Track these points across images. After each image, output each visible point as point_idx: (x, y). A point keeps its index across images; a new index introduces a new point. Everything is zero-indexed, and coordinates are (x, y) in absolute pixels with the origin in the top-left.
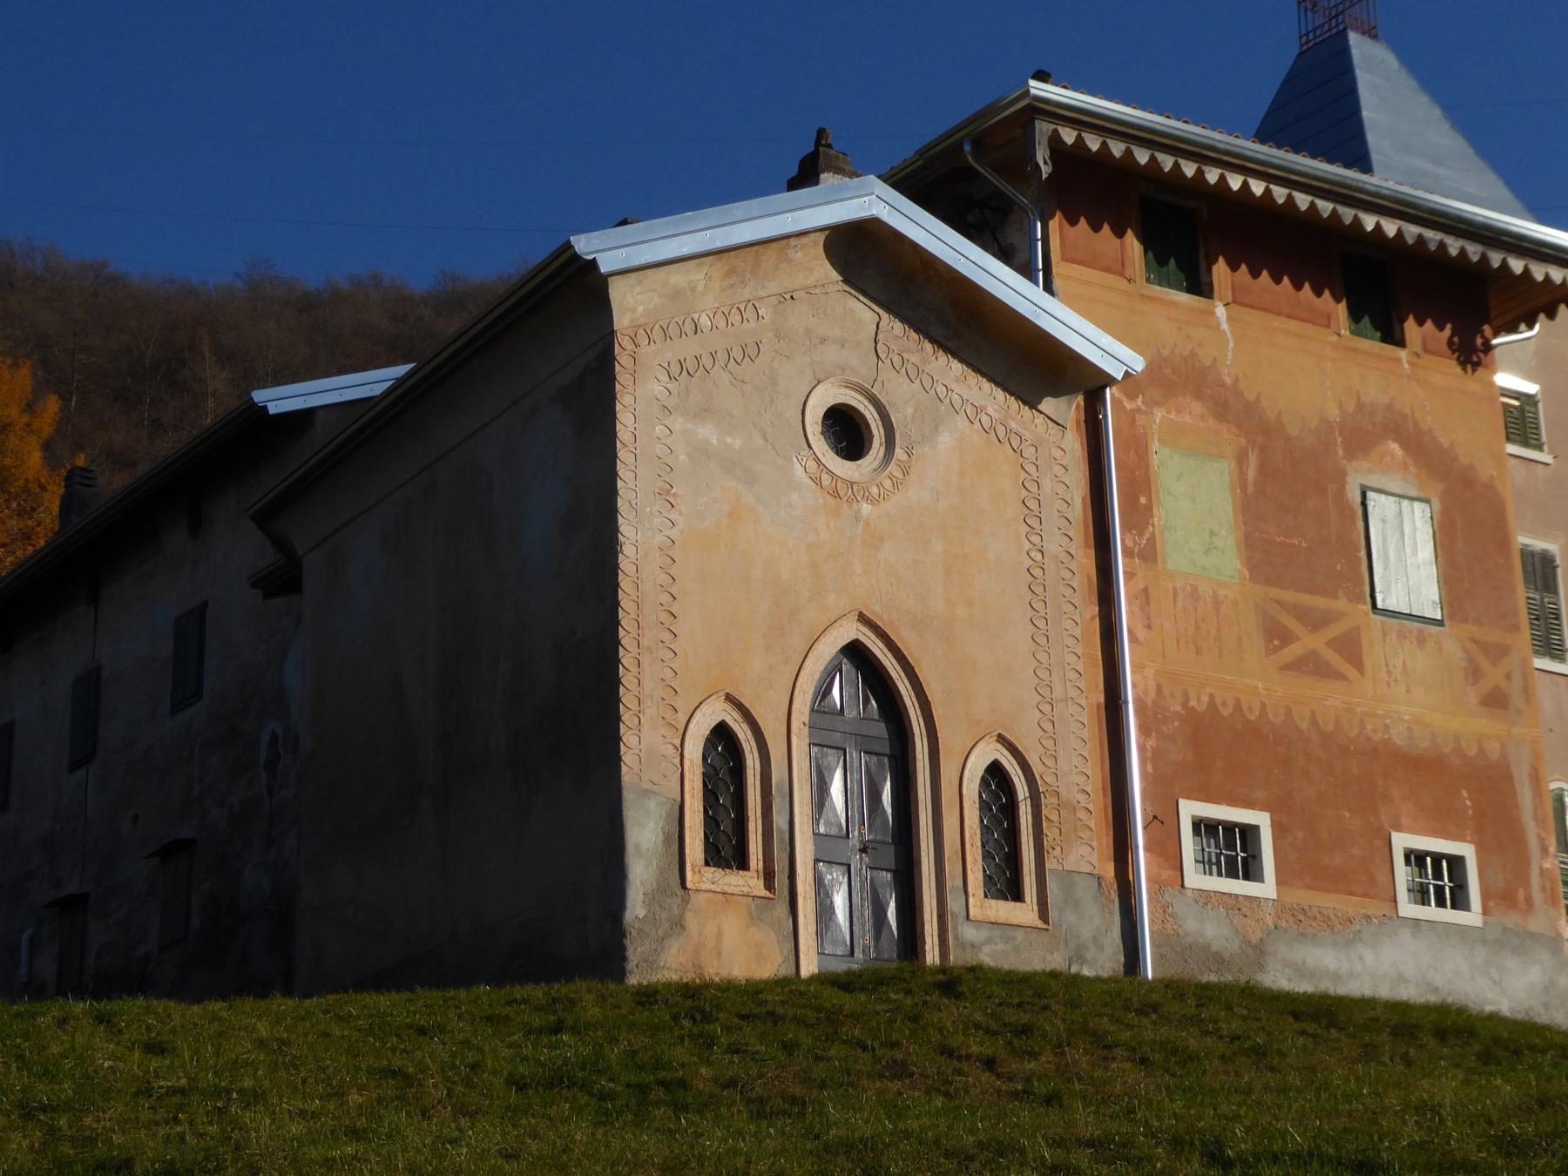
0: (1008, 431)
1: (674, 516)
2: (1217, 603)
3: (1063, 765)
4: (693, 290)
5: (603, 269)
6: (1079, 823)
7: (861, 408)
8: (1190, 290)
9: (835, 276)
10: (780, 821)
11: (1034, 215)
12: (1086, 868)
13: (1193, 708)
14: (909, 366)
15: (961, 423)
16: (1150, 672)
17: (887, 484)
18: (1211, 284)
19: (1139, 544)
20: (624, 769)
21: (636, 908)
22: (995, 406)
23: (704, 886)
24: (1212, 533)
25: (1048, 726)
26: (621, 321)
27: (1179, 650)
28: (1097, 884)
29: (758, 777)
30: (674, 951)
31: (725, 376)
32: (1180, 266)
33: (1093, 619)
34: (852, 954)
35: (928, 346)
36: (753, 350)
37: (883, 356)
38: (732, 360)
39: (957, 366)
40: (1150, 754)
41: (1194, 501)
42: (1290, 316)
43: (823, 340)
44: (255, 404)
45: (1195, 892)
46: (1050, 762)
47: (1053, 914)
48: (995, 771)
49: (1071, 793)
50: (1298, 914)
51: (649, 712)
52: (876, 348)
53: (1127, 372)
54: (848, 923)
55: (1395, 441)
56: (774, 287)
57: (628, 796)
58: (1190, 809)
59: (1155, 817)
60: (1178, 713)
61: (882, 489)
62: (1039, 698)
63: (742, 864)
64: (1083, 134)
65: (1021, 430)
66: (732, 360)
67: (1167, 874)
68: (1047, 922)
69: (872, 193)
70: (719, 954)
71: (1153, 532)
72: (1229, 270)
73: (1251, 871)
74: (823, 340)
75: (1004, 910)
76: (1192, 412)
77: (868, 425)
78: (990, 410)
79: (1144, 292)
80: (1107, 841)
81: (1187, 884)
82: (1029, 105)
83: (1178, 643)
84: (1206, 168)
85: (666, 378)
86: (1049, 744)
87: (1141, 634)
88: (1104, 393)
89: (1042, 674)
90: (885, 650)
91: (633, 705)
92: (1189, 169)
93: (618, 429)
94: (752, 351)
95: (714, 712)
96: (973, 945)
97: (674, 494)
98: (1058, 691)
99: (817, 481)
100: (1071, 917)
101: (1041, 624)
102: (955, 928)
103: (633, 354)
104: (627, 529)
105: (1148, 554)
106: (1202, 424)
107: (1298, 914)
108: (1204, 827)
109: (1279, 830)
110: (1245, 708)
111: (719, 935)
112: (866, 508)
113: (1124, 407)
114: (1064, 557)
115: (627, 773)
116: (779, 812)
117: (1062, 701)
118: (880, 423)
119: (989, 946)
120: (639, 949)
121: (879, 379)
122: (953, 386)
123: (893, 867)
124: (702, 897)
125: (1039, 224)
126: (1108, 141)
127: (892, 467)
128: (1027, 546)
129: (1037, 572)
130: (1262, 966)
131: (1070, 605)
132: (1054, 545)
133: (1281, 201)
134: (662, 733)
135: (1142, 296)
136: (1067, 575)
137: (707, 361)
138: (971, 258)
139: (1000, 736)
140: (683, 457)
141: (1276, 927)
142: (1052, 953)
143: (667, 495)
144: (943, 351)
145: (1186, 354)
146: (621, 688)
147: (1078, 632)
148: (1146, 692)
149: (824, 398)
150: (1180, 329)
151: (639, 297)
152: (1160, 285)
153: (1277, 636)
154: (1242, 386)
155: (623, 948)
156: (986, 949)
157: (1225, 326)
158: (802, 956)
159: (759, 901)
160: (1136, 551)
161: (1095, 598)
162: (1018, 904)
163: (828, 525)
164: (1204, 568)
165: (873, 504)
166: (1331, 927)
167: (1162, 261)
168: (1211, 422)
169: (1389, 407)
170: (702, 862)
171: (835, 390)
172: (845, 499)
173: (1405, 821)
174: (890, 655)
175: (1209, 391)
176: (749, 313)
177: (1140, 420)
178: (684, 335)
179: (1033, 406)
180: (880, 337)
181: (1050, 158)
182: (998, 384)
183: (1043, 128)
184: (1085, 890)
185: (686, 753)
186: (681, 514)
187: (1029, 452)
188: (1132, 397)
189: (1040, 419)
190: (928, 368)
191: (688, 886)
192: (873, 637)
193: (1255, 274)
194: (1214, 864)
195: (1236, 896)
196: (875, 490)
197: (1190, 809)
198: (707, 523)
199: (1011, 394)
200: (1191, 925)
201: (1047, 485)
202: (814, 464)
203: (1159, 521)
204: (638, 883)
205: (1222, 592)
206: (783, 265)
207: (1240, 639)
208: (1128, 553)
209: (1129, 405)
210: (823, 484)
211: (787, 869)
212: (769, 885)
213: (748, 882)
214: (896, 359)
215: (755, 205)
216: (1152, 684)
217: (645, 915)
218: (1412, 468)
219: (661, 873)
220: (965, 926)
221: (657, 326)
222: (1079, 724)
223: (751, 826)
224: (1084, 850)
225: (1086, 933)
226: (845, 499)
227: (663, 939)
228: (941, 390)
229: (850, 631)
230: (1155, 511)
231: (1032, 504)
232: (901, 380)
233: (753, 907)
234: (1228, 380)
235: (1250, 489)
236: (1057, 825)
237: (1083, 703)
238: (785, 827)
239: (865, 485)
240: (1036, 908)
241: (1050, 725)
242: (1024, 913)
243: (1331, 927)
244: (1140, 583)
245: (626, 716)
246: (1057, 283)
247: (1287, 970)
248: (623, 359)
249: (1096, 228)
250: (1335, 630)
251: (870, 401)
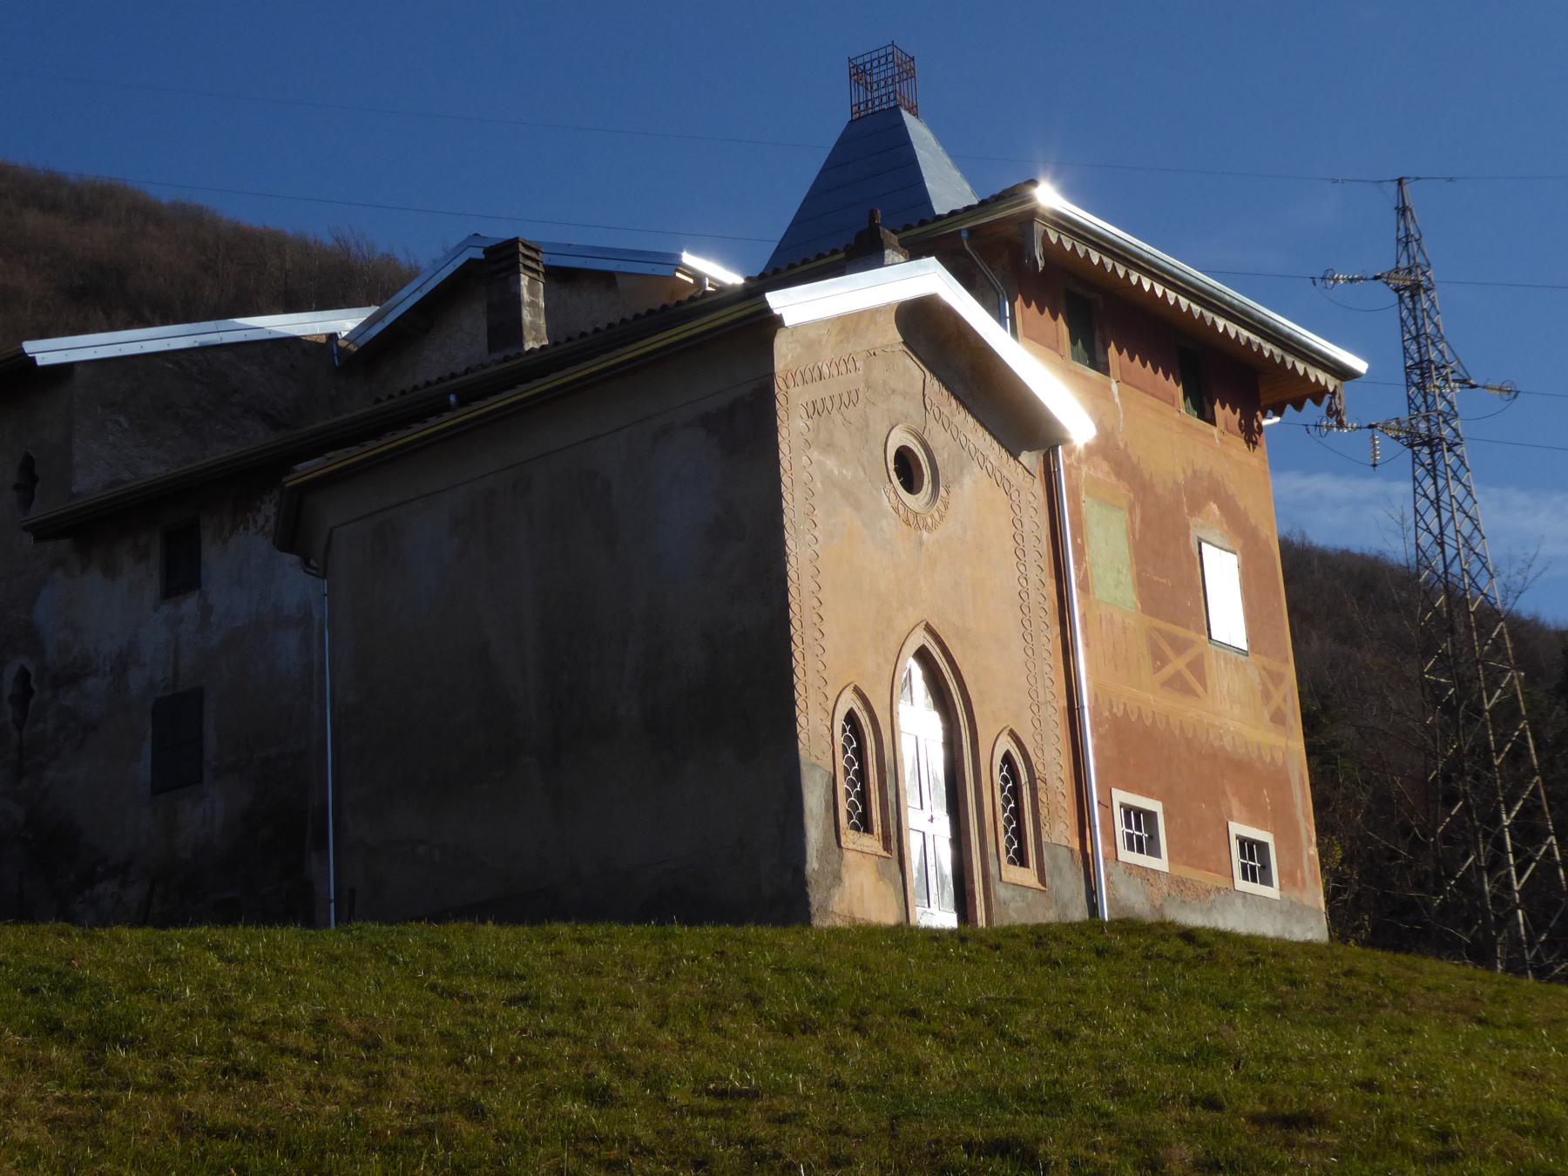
0: (1002, 477)
2: (1125, 629)
4: (820, 342)
7: (916, 450)
11: (1003, 296)
12: (1064, 842)
20: (800, 745)
21: (813, 864)
31: (839, 417)
33: (1057, 637)
36: (852, 398)
37: (929, 408)
42: (1152, 395)
44: (24, 354)
46: (1040, 754)
47: (1048, 879)
55: (1214, 502)
57: (804, 768)
65: (1010, 478)
78: (991, 459)
81: (1120, 858)
84: (1130, 271)
95: (849, 702)
98: (1041, 699)
99: (896, 510)
102: (994, 888)
118: (927, 464)
121: (928, 427)
125: (1007, 304)
132: (1034, 574)
147: (1049, 647)
149: (899, 438)
153: (1159, 659)
155: (806, 895)
159: (882, 859)
161: (1058, 622)
169: (1210, 474)
173: (1235, 813)
176: (851, 365)
182: (995, 438)
197: (1120, 796)
212: (887, 847)
213: (872, 843)
214: (936, 411)
218: (1225, 526)
219: (825, 833)
221: (798, 371)
234: (1122, 445)
235: (1137, 537)
238: (894, 800)
250: (1190, 655)
251: (921, 445)
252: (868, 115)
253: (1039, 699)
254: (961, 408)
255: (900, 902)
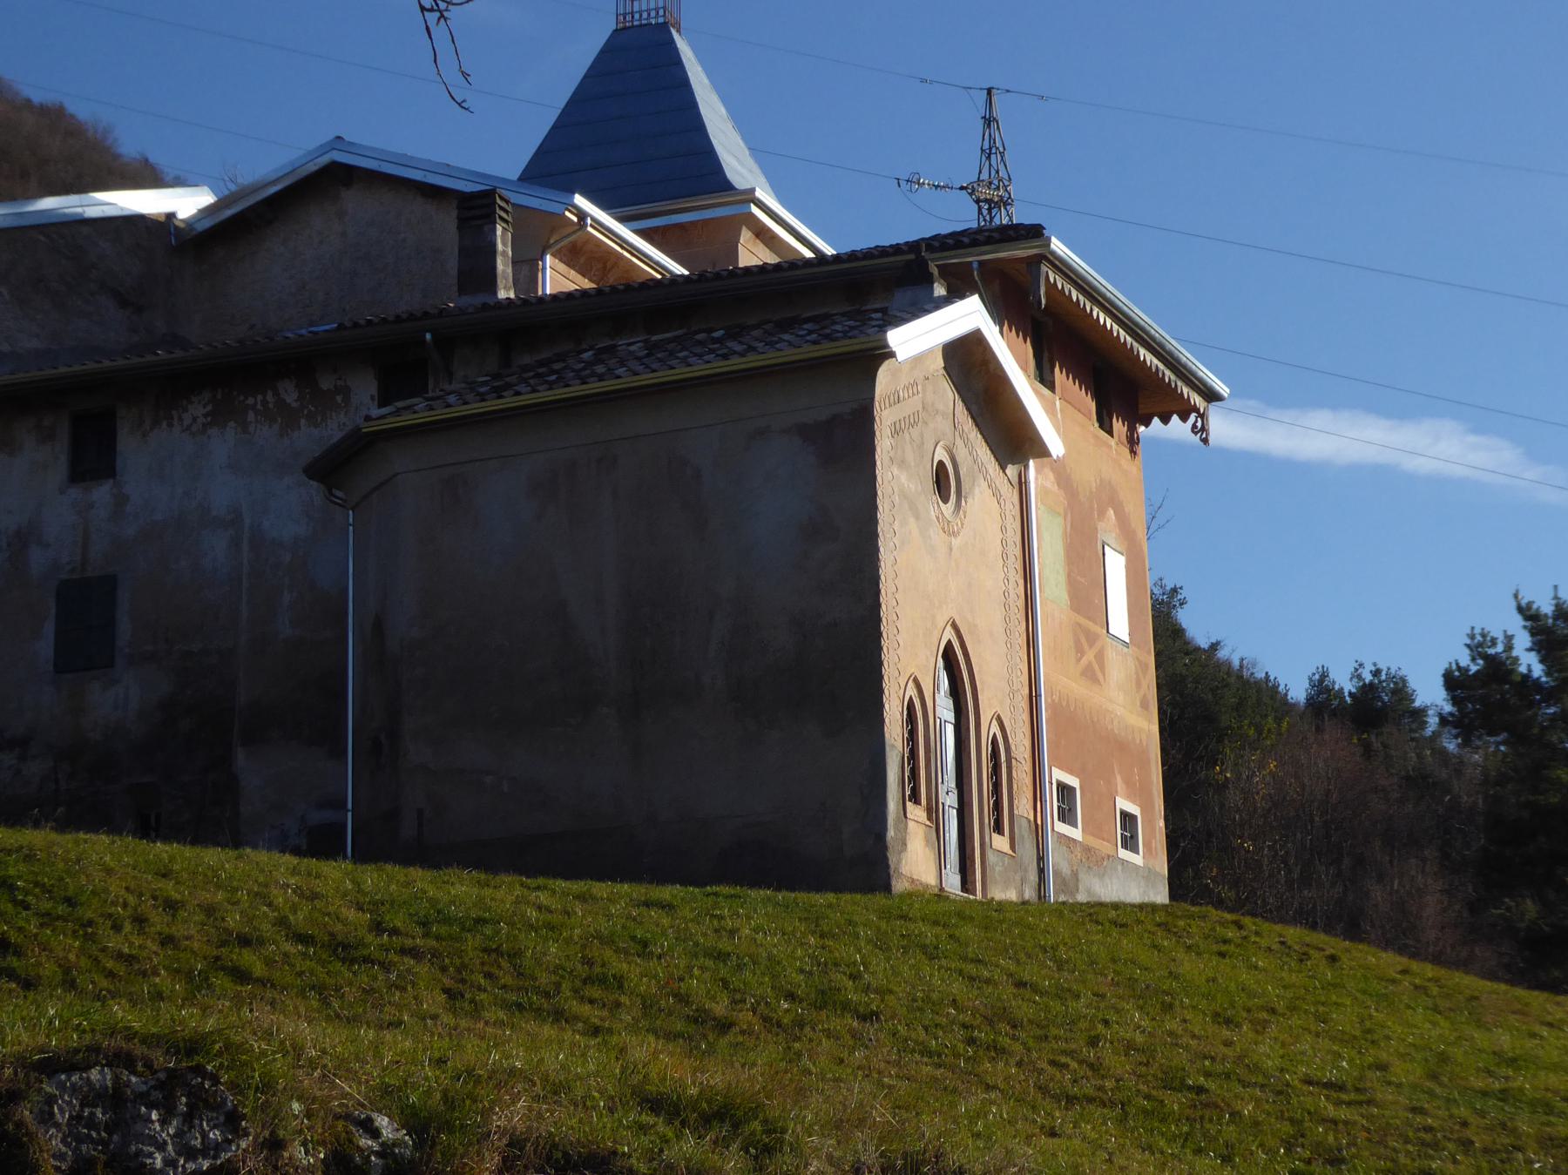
7: (947, 464)
46: (1013, 737)
57: (888, 748)
99: (938, 518)
149: (941, 455)
155: (886, 859)
212: (929, 818)
252: (633, 26)
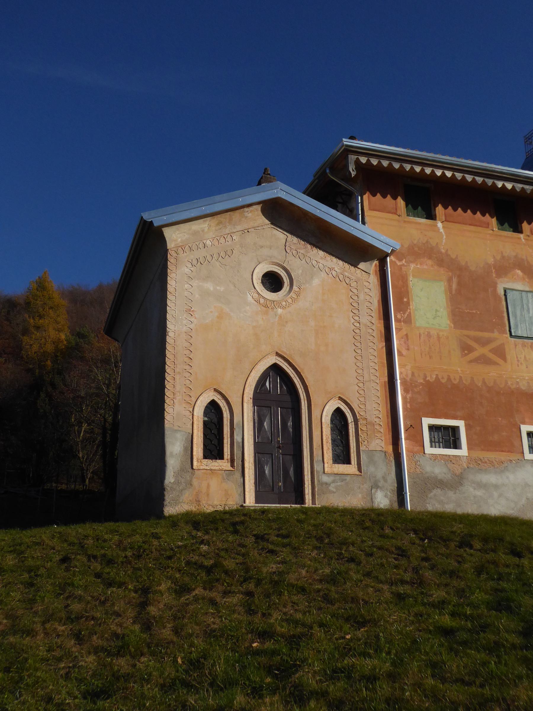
1: (192, 319)
2: (439, 338)
3: (368, 407)
4: (203, 231)
5: (156, 224)
6: (376, 430)
7: (279, 272)
8: (427, 218)
9: (267, 222)
10: (237, 438)
12: (379, 449)
13: (429, 380)
14: (300, 254)
15: (323, 275)
16: (408, 367)
17: (290, 301)
18: (435, 215)
19: (404, 317)
20: (166, 422)
21: (170, 478)
22: (339, 267)
23: (201, 467)
24: (437, 311)
25: (362, 392)
26: (170, 245)
27: (422, 357)
28: (384, 455)
29: (229, 421)
30: (187, 495)
31: (218, 264)
32: (423, 209)
33: (382, 348)
34: (273, 490)
35: (309, 246)
36: (229, 253)
38: (220, 257)
39: (321, 253)
40: (408, 400)
41: (428, 299)
42: (470, 225)
43: (262, 247)
45: (430, 455)
47: (363, 468)
48: (338, 412)
49: (371, 418)
50: (478, 462)
51: (179, 397)
52: (285, 248)
53: (392, 250)
54: (271, 477)
55: (518, 269)
56: (239, 228)
57: (167, 433)
58: (427, 422)
59: (411, 426)
60: (421, 383)
61: (287, 303)
62: (358, 381)
63: (221, 457)
64: (370, 159)
66: (220, 257)
67: (416, 449)
68: (361, 472)
69: (278, 188)
70: (208, 495)
71: (410, 312)
72: (443, 209)
73: (456, 445)
74: (262, 247)
75: (342, 468)
76: (428, 264)
77: (282, 278)
78: (336, 269)
79: (406, 220)
80: (389, 437)
81: (426, 452)
82: (345, 148)
83: (421, 355)
84: (425, 168)
85: (191, 266)
86: (362, 399)
87: (404, 352)
88: (387, 259)
89: (360, 371)
90: (288, 366)
91: (171, 396)
92: (418, 169)
93: (168, 287)
94: (229, 253)
96: (326, 484)
97: (193, 311)
99: (258, 302)
100: (372, 469)
101: (359, 351)
102: (318, 477)
103: (176, 257)
104: (171, 326)
105: (408, 321)
106: (432, 269)
107: (478, 462)
108: (432, 428)
109: (468, 427)
110: (452, 378)
111: (208, 486)
112: (280, 311)
113: (397, 264)
114: (369, 324)
115: (167, 423)
116: (237, 435)
117: (368, 381)
118: (287, 277)
119: (333, 484)
120: (171, 496)
122: (320, 261)
123: (293, 454)
124: (199, 472)
125: (360, 197)
126: (381, 160)
127: (292, 294)
128: (353, 321)
129: (357, 331)
130: (462, 484)
131: (372, 343)
132: (365, 320)
133: (459, 178)
134: (184, 406)
135: (405, 221)
136: (371, 331)
137: (209, 258)
138: (323, 210)
139: (339, 397)
140: (197, 296)
141: (468, 467)
142: (363, 484)
143: (190, 312)
144: (316, 247)
145: (424, 242)
146: (166, 389)
147: (375, 354)
148: (407, 375)
150: (421, 232)
151: (178, 235)
152: (414, 217)
153: (466, 349)
154: (449, 252)
155: (164, 495)
156: (333, 485)
157: (442, 230)
158: (246, 493)
159: (227, 472)
160: (402, 320)
161: (383, 339)
162: (348, 465)
163: (263, 318)
164: (433, 324)
165: (283, 309)
166: (494, 466)
167: (415, 208)
168: (436, 267)
169: (516, 257)
170: (202, 457)
171: (267, 266)
172: (270, 308)
173: (527, 420)
174: (290, 368)
175: (435, 256)
176: (229, 238)
177: (404, 269)
178: (199, 249)
179: (355, 266)
180: (287, 244)
181: (356, 169)
182: (340, 259)
183: (352, 158)
184: (379, 458)
185: (195, 414)
186: (195, 318)
187: (354, 284)
188: (400, 260)
189: (358, 271)
190: (308, 255)
191: (194, 468)
192: (283, 361)
193: (455, 210)
194: (437, 442)
195: (449, 456)
196: (284, 303)
197: (427, 422)
198: (207, 321)
199: (346, 262)
200: (428, 469)
201: (362, 296)
202: (257, 295)
203: (413, 307)
204: (171, 468)
205: (441, 334)
206: (243, 219)
207: (449, 352)
208: (397, 320)
209: (399, 263)
210: (261, 303)
211: (241, 457)
212: (232, 465)
213: (224, 464)
214: (294, 252)
215: (225, 196)
216: (410, 372)
217: (174, 481)
218: (527, 280)
220: (323, 476)
221: (187, 247)
222: (376, 390)
223: (225, 441)
224: (378, 441)
225: (379, 475)
226: (270, 308)
227: (182, 491)
228: (314, 263)
229: (273, 360)
230: (411, 303)
231: (355, 304)
232: (296, 260)
233: (224, 474)
234: (443, 251)
235: (454, 292)
236: (366, 432)
237: (378, 381)
238: (240, 440)
239: (279, 302)
240: (356, 466)
241: (363, 391)
242: (351, 469)
243: (494, 466)
244: (404, 332)
245: (167, 401)
246: (367, 219)
247: (473, 485)
248: (171, 259)
249: (384, 197)
250: (493, 345)
251: (283, 269)
253: (364, 380)
254: (314, 248)
255: (239, 492)
